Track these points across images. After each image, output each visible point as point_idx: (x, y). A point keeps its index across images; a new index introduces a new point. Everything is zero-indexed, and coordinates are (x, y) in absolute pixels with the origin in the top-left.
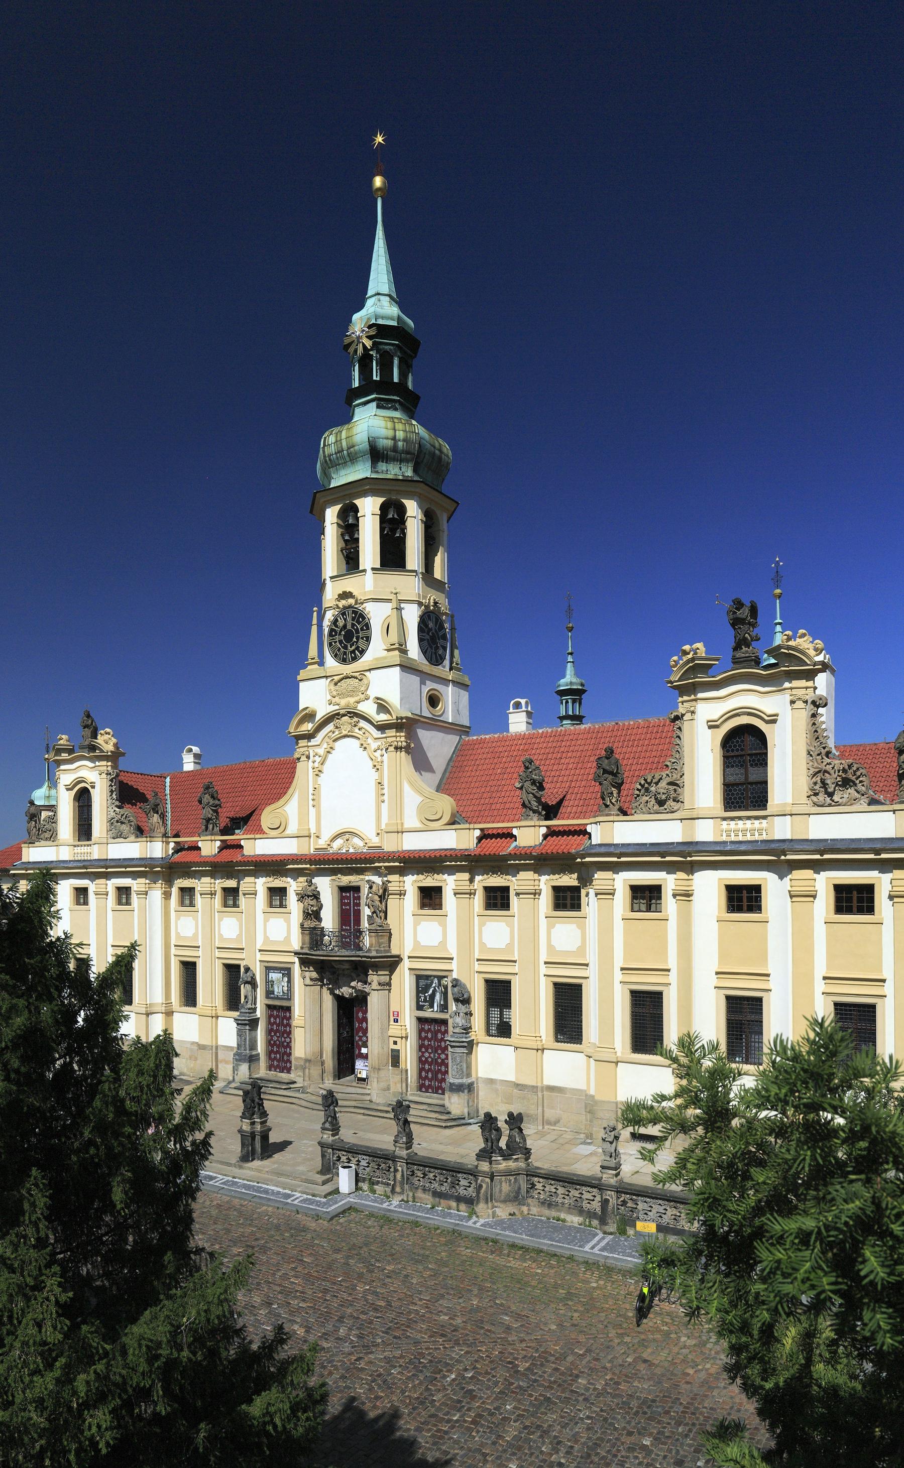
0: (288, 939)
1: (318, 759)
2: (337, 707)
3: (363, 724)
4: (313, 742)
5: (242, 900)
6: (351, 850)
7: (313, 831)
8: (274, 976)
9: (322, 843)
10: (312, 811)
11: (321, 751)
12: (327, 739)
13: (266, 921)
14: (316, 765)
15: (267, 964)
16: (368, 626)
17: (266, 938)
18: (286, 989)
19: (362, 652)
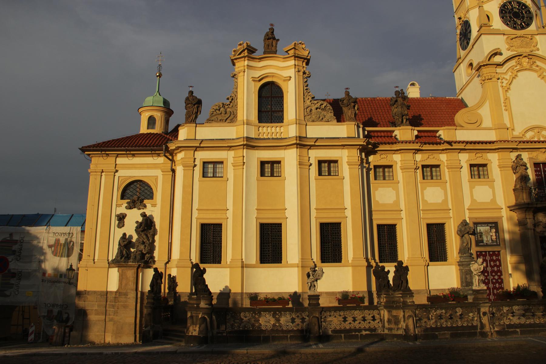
0: (494, 200)
1: (505, 82)
2: (516, 52)
3: (538, 63)
4: (499, 70)
5: (446, 173)
6: (542, 139)
7: (508, 126)
8: (481, 229)
9: (516, 133)
10: (506, 114)
11: (507, 77)
12: (510, 70)
13: (471, 188)
14: (504, 85)
15: (476, 221)
16: (530, 12)
17: (473, 200)
18: (494, 237)
19: (528, 25)
